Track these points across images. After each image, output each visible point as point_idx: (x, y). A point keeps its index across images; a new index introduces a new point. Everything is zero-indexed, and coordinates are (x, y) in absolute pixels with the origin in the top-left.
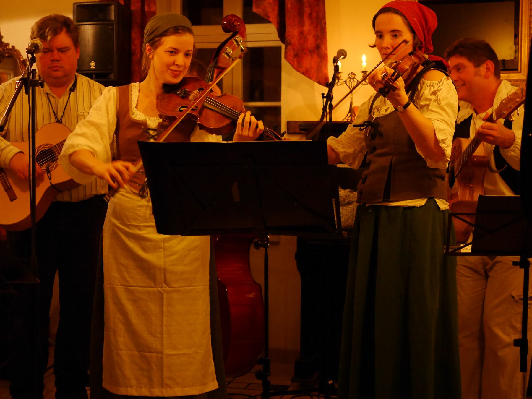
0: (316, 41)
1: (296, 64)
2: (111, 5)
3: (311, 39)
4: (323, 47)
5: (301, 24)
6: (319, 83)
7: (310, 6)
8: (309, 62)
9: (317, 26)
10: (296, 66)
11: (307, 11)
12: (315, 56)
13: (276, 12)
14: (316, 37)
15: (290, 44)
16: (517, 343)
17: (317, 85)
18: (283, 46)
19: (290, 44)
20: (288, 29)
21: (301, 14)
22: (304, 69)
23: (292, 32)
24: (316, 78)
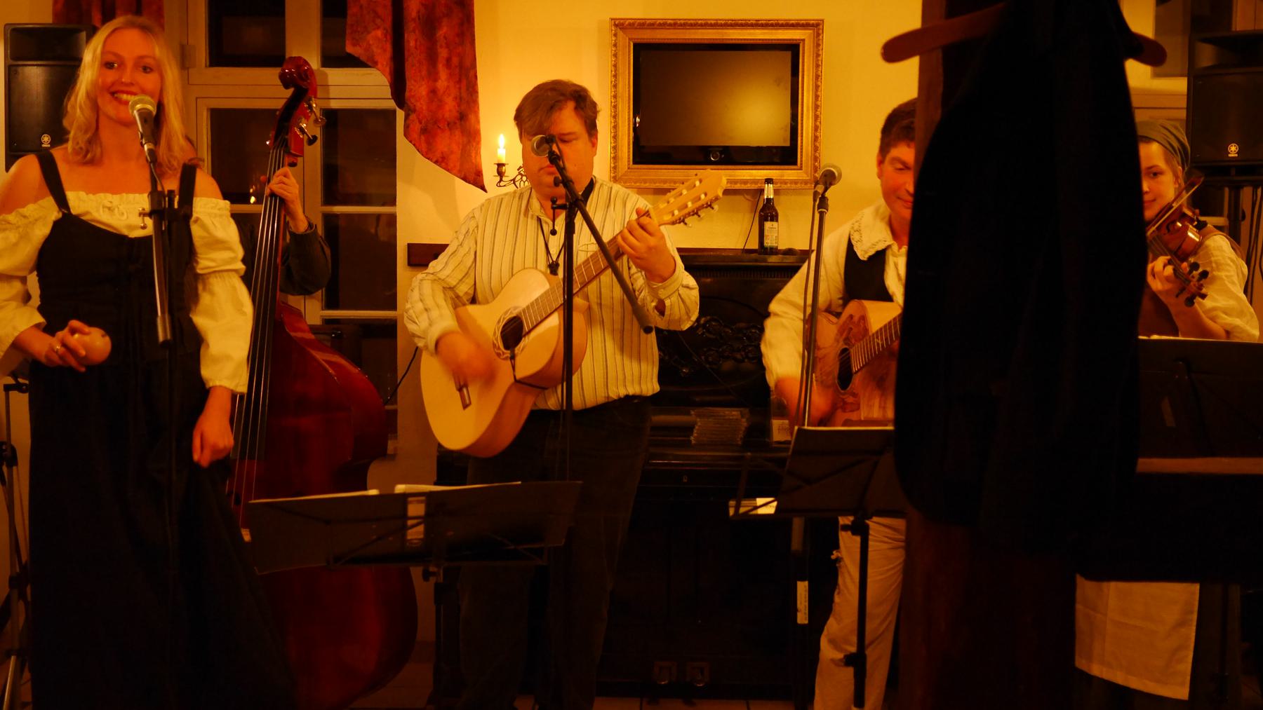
0: (459, 106)
1: (424, 146)
2: (81, 31)
3: (450, 105)
4: (472, 117)
5: (433, 76)
6: (465, 179)
7: (448, 46)
8: (445, 143)
9: (460, 81)
10: (424, 150)
11: (443, 53)
12: (457, 133)
13: (388, 54)
14: (459, 100)
15: (414, 111)
16: (850, 660)
17: (459, 183)
18: (400, 114)
19: (414, 111)
20: (410, 84)
21: (432, 59)
22: (438, 155)
23: (418, 89)
24: (460, 171)
